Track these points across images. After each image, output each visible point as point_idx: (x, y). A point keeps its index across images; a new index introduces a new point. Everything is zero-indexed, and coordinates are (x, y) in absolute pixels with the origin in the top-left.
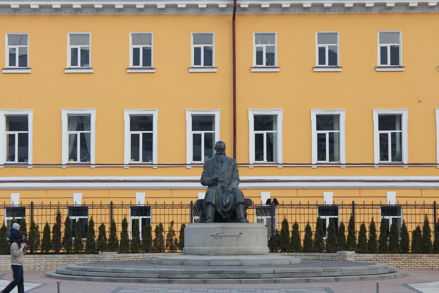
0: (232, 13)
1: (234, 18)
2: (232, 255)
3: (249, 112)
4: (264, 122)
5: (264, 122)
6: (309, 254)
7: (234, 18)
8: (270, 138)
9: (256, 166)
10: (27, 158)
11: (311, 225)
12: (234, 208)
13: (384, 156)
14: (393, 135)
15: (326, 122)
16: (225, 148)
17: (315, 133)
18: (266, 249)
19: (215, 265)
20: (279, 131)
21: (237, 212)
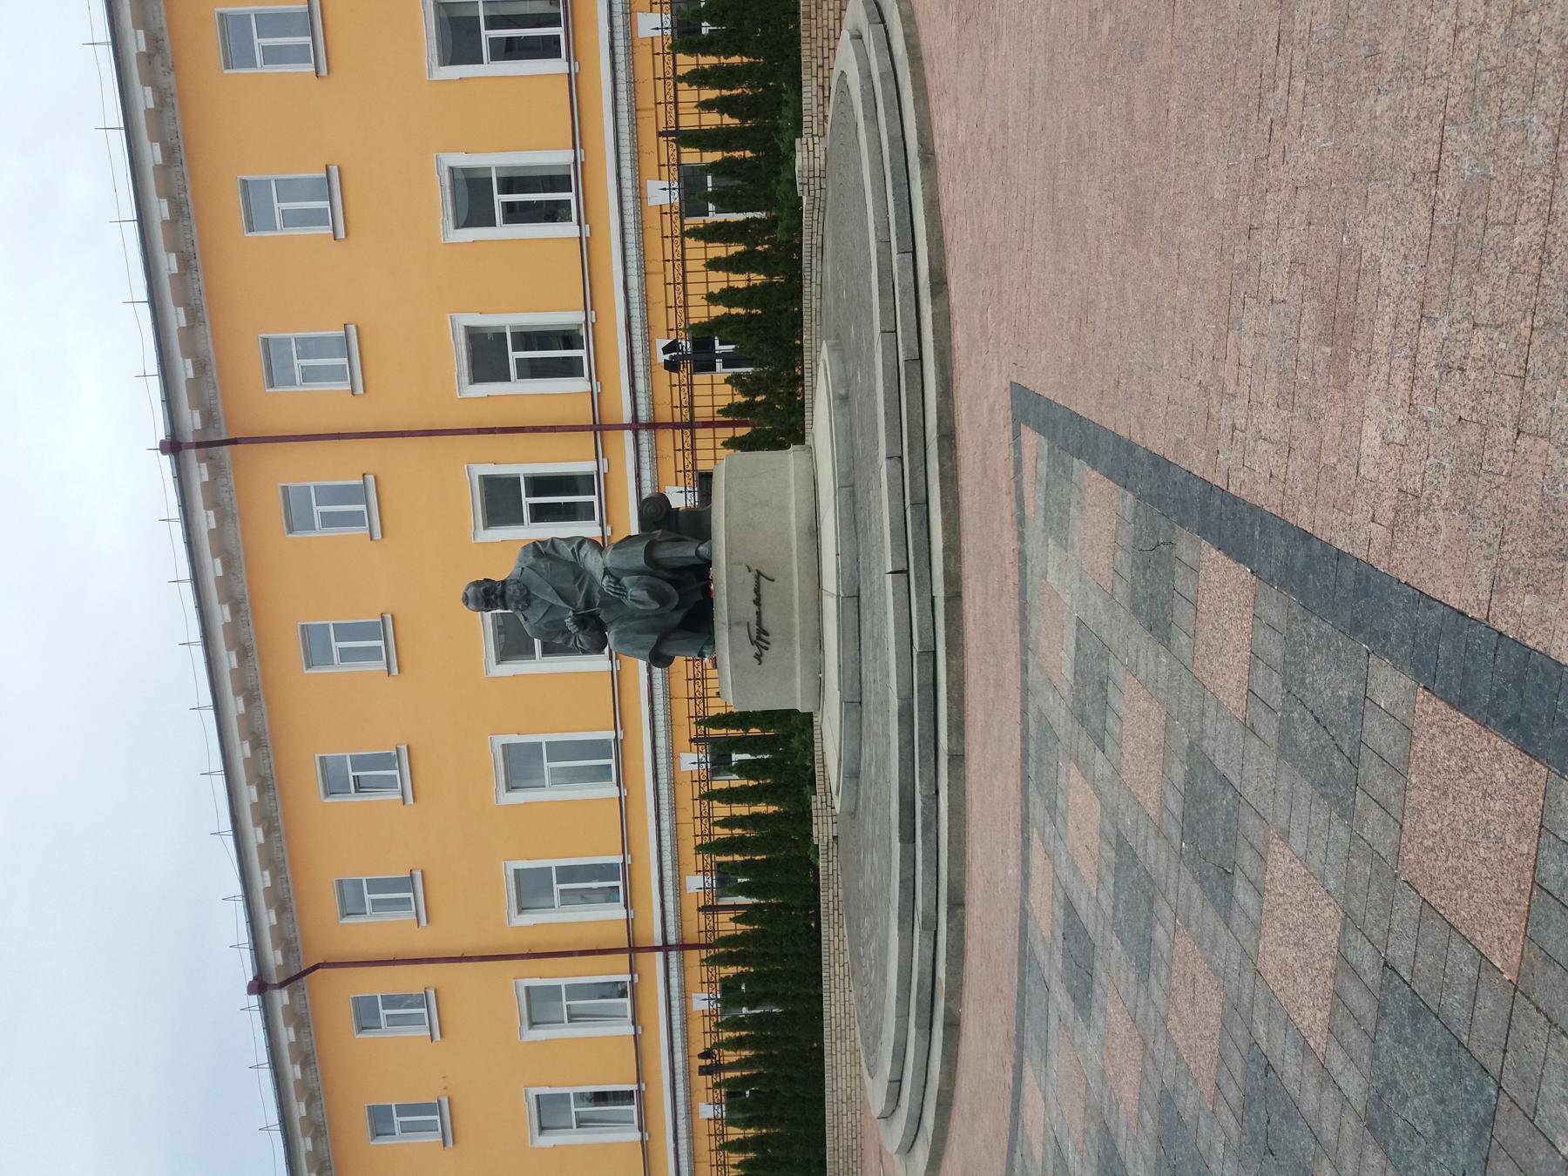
0: (225, 448)
1: (234, 441)
2: (819, 600)
3: (465, 395)
4: (487, 355)
5: (487, 355)
6: (806, 274)
7: (234, 441)
8: (528, 339)
9: (596, 376)
10: (610, 865)
11: (715, 289)
12: (665, 574)
13: (548, 48)
14: (493, 23)
15: (474, 199)
16: (487, 580)
17: (503, 231)
18: (791, 458)
19: (857, 684)
20: (509, 321)
21: (679, 564)
